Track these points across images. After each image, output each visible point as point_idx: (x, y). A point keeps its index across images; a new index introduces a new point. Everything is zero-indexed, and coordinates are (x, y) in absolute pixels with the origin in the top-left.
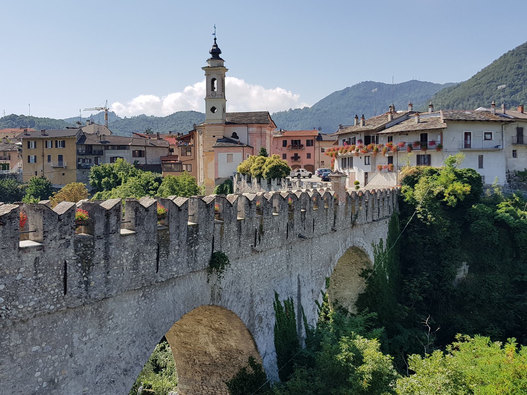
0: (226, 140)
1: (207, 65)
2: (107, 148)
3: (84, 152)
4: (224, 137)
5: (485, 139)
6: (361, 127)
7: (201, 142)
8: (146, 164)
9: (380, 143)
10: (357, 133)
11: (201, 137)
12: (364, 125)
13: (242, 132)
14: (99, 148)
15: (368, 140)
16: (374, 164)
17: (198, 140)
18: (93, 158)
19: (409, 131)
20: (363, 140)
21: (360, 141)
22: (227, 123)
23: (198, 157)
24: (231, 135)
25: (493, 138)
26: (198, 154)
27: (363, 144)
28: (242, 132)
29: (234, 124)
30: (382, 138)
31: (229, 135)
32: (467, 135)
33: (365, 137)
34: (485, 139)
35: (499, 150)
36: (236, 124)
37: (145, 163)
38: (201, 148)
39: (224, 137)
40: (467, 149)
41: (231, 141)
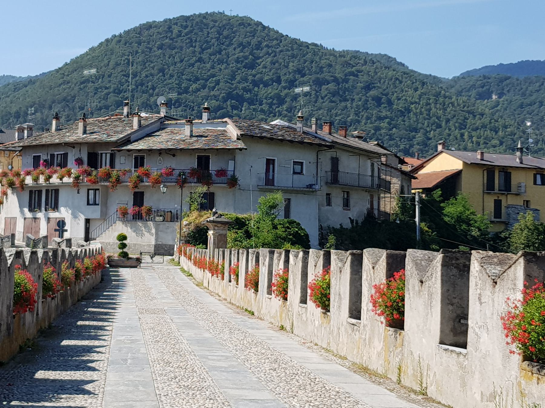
5: (295, 173)
6: (77, 134)
9: (118, 166)
10: (72, 145)
12: (85, 132)
15: (93, 161)
16: (105, 206)
19: (176, 149)
20: (85, 159)
21: (79, 162)
25: (304, 172)
27: (85, 167)
30: (123, 159)
32: (270, 163)
34: (295, 173)
35: (313, 192)
40: (270, 187)
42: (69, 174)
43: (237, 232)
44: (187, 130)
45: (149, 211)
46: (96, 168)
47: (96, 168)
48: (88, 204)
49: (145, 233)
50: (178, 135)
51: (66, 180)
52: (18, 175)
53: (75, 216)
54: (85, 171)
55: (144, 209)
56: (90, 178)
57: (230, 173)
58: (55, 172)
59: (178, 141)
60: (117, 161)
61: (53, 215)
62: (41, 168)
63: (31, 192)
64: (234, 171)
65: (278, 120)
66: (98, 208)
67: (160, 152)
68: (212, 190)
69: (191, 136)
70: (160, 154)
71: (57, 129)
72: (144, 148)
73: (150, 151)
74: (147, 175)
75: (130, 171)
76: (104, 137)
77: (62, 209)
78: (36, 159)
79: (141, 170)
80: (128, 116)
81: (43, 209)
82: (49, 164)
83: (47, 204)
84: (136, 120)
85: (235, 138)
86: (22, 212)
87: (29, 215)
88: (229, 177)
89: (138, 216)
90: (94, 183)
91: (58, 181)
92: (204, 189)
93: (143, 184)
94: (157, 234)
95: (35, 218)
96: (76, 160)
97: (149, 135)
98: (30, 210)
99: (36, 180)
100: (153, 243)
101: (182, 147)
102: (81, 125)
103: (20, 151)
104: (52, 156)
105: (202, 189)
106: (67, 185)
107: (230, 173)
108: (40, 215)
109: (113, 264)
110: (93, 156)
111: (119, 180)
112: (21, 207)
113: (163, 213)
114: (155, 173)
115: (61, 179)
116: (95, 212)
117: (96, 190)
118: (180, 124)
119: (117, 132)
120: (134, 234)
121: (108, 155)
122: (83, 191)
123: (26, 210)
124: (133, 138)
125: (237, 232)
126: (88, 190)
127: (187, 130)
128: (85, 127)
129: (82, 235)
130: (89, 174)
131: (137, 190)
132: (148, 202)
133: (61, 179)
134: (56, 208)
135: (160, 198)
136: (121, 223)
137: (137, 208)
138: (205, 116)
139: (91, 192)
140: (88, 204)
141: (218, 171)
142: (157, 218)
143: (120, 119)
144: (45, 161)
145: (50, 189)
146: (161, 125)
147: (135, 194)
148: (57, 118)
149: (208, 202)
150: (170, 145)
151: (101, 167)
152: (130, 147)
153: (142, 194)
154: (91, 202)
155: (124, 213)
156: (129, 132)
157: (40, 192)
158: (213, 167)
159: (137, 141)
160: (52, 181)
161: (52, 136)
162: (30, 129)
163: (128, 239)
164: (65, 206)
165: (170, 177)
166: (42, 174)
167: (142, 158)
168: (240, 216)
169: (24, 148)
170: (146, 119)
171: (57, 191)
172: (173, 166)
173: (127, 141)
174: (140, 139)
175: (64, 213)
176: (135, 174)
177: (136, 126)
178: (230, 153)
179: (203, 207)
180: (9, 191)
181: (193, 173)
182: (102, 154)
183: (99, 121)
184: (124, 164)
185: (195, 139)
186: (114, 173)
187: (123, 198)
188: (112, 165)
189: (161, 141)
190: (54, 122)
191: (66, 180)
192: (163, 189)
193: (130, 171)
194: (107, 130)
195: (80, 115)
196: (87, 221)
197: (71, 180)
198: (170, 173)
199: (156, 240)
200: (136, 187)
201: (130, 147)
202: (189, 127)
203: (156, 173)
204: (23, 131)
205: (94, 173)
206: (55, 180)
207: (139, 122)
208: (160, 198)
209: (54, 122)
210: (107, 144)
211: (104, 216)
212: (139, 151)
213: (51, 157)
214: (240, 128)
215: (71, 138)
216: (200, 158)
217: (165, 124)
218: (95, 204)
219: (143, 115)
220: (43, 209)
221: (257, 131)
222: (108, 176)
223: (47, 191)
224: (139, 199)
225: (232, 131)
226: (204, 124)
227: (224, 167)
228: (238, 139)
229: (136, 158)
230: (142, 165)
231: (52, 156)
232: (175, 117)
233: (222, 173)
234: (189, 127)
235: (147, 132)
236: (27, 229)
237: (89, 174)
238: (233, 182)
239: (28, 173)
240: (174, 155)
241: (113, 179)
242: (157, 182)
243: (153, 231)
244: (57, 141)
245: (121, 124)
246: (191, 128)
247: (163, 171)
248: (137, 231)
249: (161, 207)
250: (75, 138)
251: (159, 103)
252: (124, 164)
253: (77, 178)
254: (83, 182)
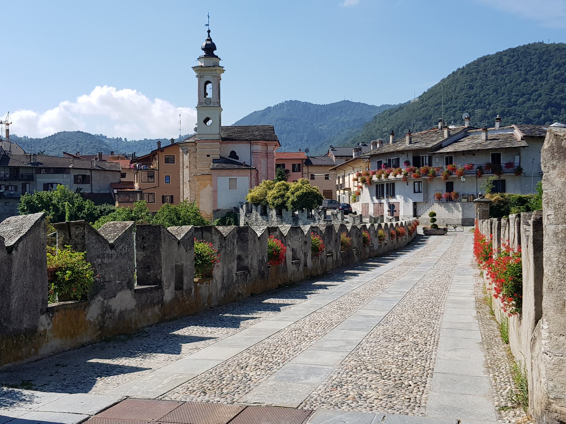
0: (222, 160)
1: (199, 64)
2: (39, 171)
3: (8, 176)
4: (221, 157)
6: (405, 144)
7: (187, 163)
8: (92, 193)
10: (402, 152)
11: (186, 157)
12: (410, 143)
13: (243, 151)
14: (29, 172)
15: (417, 162)
16: (426, 193)
17: (181, 160)
18: (19, 184)
21: (407, 163)
22: (224, 140)
23: (181, 182)
24: (229, 154)
26: (181, 179)
27: (411, 166)
28: (243, 151)
29: (232, 140)
31: (227, 154)
33: (414, 158)
36: (235, 140)
37: (90, 192)
38: (186, 171)
39: (221, 157)
41: (230, 162)
42: (400, 172)
43: (519, 208)
44: (483, 136)
45: (457, 195)
46: (419, 167)
47: (419, 167)
48: (415, 192)
49: (455, 211)
50: (479, 139)
51: (398, 176)
52: (368, 175)
53: (406, 201)
54: (411, 170)
55: (453, 194)
56: (414, 174)
57: (516, 165)
58: (391, 171)
59: (477, 144)
60: (433, 161)
61: (392, 201)
62: (383, 169)
63: (377, 186)
64: (520, 163)
65: (556, 123)
66: (421, 194)
67: (464, 153)
68: (502, 177)
69: (487, 140)
70: (464, 154)
71: (393, 142)
72: (451, 151)
73: (456, 153)
74: (454, 169)
75: (442, 168)
76: (423, 145)
77: (397, 196)
78: (380, 163)
79: (450, 166)
80: (441, 128)
81: (385, 196)
82: (387, 166)
83: (387, 194)
84: (446, 131)
85: (520, 139)
86: (372, 199)
87: (376, 201)
88: (516, 168)
89: (449, 199)
90: (417, 177)
91: (393, 177)
92: (495, 177)
93: (452, 176)
94: (463, 211)
95: (381, 203)
96: (405, 163)
97: (456, 141)
98: (377, 198)
99: (379, 177)
100: (461, 217)
101: (479, 148)
102: (407, 138)
103: (369, 158)
104: (390, 160)
105: (495, 177)
106: (399, 180)
107: (516, 165)
108: (384, 201)
109: (427, 233)
110: (417, 158)
111: (434, 175)
112: (371, 196)
113: (466, 196)
114: (460, 168)
115: (395, 176)
116: (419, 198)
117: (419, 182)
118: (479, 132)
119: (433, 141)
120: (447, 212)
121: (427, 157)
122: (411, 184)
123: (374, 198)
124: (444, 144)
125: (519, 208)
126: (414, 182)
127: (483, 136)
128: (410, 139)
129: (411, 213)
130: (414, 172)
131: (447, 181)
132: (457, 189)
133: (395, 176)
134: (393, 196)
135: (463, 185)
136: (437, 204)
137: (448, 194)
138: (497, 124)
139: (416, 183)
140: (415, 192)
141: (506, 164)
142: (463, 200)
143: (436, 131)
144: (385, 164)
145: (389, 183)
146: (465, 134)
147: (447, 184)
148: (393, 134)
149: (499, 187)
150: (470, 148)
151: (423, 166)
152: (441, 151)
153: (452, 183)
154: (417, 190)
155: (439, 198)
156: (441, 140)
157: (383, 185)
158: (504, 161)
159: (447, 146)
160: (389, 177)
161: (390, 147)
162: (381, 142)
163: (437, 215)
164: (399, 194)
165: (471, 170)
166: (383, 173)
167: (451, 158)
168: (523, 196)
169: (371, 156)
170: (454, 130)
171: (393, 184)
172: (473, 163)
173: (440, 146)
174: (449, 145)
175: (399, 199)
176: (446, 170)
177: (446, 136)
178: (517, 150)
179: (493, 191)
180: (364, 186)
181: (488, 166)
182: (423, 157)
183: (422, 134)
184: (438, 163)
185: (489, 141)
186: (431, 170)
187: (439, 187)
188: (430, 164)
189: (464, 145)
190: (391, 137)
191: (398, 176)
192: (463, 179)
193: (442, 168)
194: (425, 141)
195: (406, 131)
196: (415, 204)
197: (402, 176)
198: (471, 168)
199: (463, 215)
200: (446, 179)
201: (441, 151)
202: (484, 133)
203: (460, 168)
204: (376, 145)
205: (417, 171)
206: (391, 177)
207: (449, 132)
208: (463, 185)
209: (391, 137)
210: (425, 150)
211: (426, 200)
212: (448, 153)
213: (388, 161)
214: (523, 131)
215: (401, 147)
216: (493, 155)
217: (468, 133)
218: (420, 192)
219: (450, 127)
220: (385, 196)
221: (537, 132)
222: (427, 172)
223: (387, 184)
224: (450, 187)
225: (518, 134)
226: (497, 131)
227: (511, 161)
228: (522, 139)
229: (447, 158)
230: (451, 163)
231: (390, 160)
232: (476, 127)
233: (510, 165)
234: (484, 133)
235: (454, 139)
236: (376, 211)
237: (414, 172)
238: (519, 171)
239: (374, 173)
240: (474, 155)
241: (430, 174)
242: (461, 174)
243: (460, 209)
244: (392, 150)
245: (436, 135)
246: (487, 134)
247: (465, 166)
248: (449, 209)
249: (466, 192)
250: (403, 147)
251: (463, 118)
252: (438, 163)
253: (406, 175)
254: (410, 177)
